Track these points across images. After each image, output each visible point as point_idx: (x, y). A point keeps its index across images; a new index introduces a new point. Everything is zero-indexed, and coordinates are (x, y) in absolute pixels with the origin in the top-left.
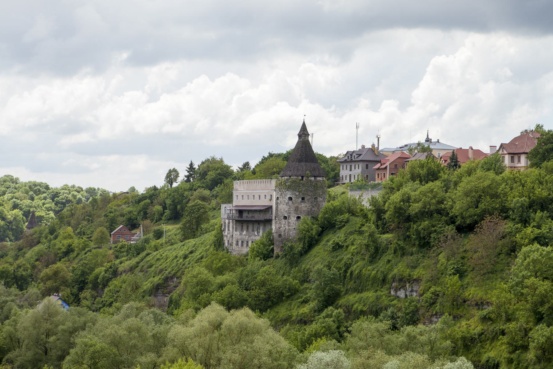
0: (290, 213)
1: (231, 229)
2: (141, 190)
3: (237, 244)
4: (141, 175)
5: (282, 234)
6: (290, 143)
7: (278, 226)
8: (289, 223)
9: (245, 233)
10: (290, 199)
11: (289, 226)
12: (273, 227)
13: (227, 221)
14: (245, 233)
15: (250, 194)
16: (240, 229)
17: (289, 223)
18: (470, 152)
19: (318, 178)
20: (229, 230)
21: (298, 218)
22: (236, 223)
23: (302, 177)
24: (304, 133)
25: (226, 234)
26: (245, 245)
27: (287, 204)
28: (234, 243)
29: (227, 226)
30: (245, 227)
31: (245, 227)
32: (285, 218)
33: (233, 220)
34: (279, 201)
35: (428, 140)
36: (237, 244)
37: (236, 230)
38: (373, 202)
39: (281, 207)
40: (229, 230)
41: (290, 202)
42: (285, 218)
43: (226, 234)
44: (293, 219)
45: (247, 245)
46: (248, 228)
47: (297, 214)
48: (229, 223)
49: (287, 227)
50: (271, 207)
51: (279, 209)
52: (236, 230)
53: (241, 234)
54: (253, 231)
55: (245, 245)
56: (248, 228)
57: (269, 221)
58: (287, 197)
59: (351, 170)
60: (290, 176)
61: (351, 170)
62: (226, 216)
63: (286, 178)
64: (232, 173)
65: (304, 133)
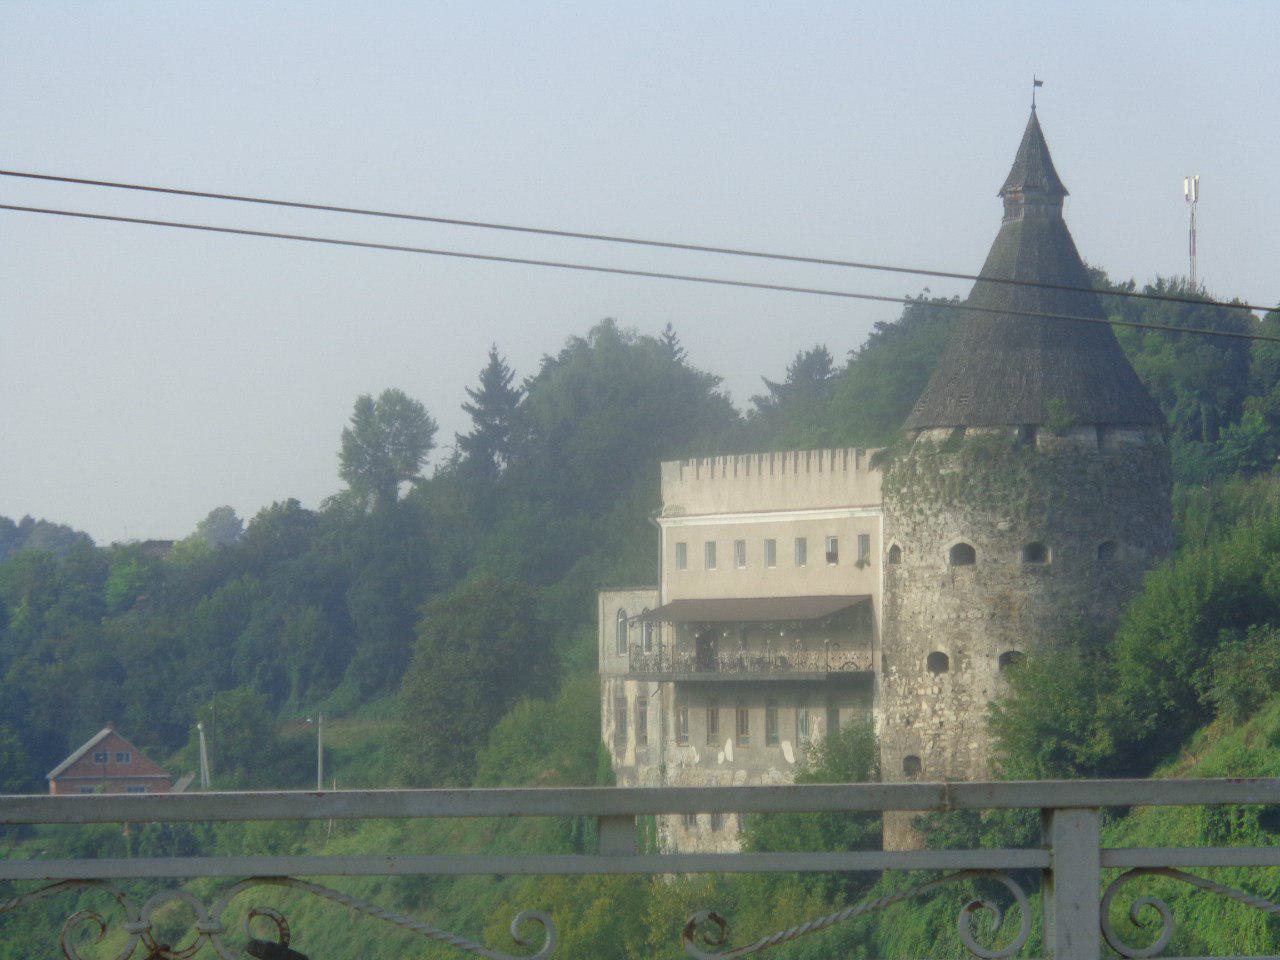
0: (961, 635)
1: (653, 733)
5: (926, 752)
6: (956, 240)
7: (899, 710)
8: (959, 689)
9: (728, 751)
10: (963, 555)
11: (961, 707)
12: (878, 715)
13: (631, 689)
14: (728, 751)
15: (739, 529)
16: (703, 730)
17: (959, 689)
20: (642, 739)
22: (678, 702)
23: (1029, 432)
25: (629, 759)
27: (947, 583)
29: (631, 716)
30: (727, 717)
31: (727, 717)
32: (938, 662)
33: (662, 681)
34: (902, 572)
37: (681, 739)
40: (642, 739)
41: (965, 575)
42: (938, 662)
43: (629, 759)
46: (742, 728)
47: (1004, 638)
48: (642, 702)
49: (950, 716)
50: (864, 604)
51: (904, 615)
52: (681, 739)
54: (772, 739)
56: (742, 728)
57: (857, 687)
58: (946, 548)
62: (623, 663)
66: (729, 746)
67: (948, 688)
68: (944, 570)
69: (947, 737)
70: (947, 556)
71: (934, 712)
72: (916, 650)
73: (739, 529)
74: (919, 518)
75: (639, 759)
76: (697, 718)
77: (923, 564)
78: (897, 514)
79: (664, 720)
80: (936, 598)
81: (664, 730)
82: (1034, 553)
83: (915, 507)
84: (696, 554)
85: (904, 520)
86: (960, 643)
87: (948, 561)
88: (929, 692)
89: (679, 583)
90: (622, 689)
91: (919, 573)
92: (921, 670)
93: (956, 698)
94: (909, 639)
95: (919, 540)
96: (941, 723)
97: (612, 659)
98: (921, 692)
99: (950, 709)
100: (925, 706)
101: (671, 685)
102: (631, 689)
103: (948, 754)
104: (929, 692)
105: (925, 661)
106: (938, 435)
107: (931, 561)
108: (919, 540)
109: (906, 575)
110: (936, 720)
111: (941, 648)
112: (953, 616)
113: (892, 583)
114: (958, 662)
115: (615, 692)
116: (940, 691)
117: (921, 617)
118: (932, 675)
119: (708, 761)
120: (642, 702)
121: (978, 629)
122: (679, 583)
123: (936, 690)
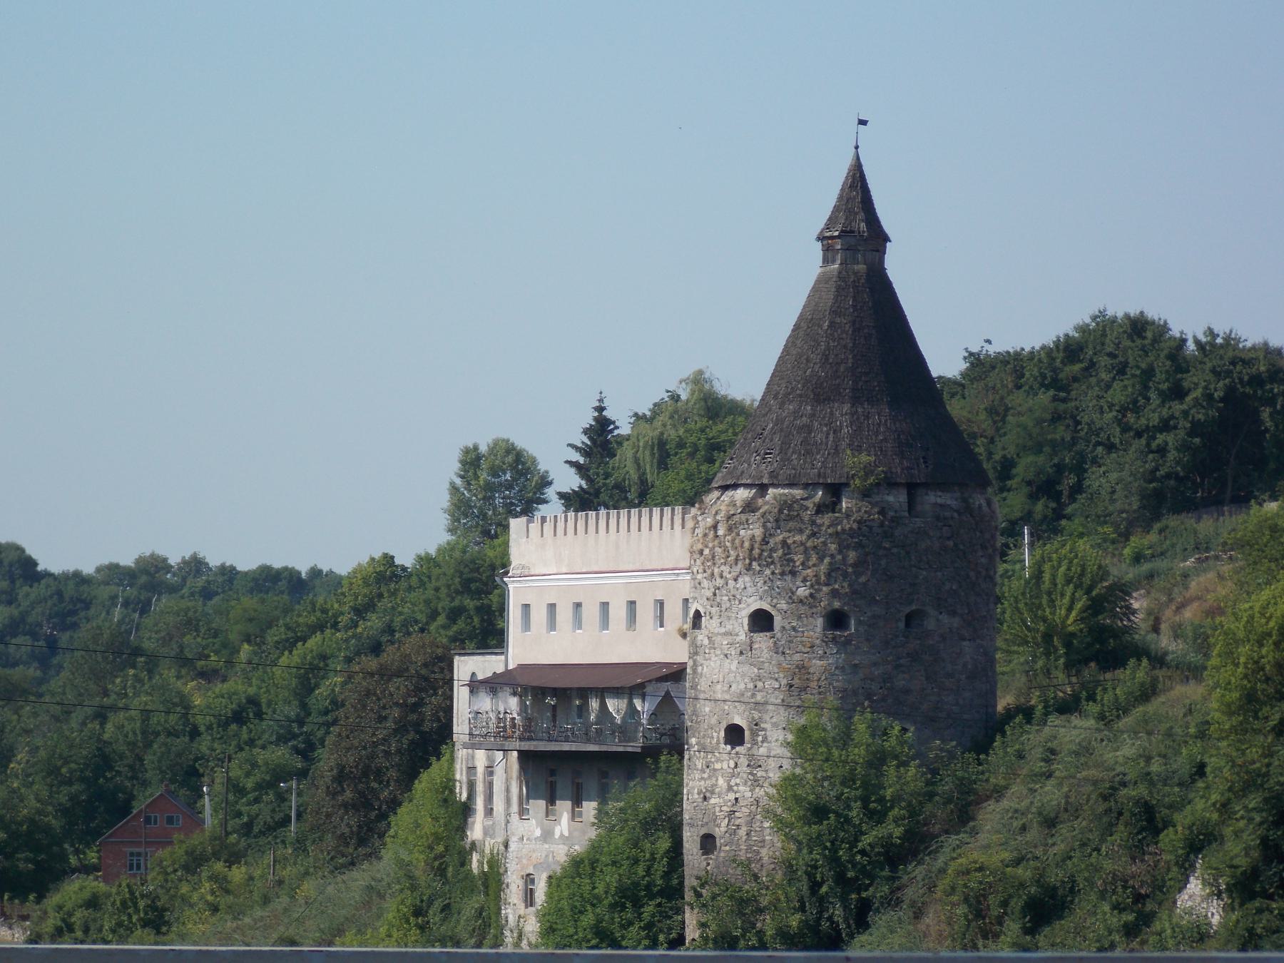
5: (719, 831)
8: (754, 764)
10: (761, 621)
11: (756, 783)
20: (489, 812)
27: (746, 651)
29: (480, 788)
32: (734, 735)
37: (522, 812)
40: (489, 812)
41: (763, 641)
48: (490, 770)
49: (744, 791)
58: (745, 613)
60: (763, 489)
63: (742, 494)
66: (565, 818)
67: (743, 761)
68: (742, 637)
69: (743, 812)
70: (746, 621)
71: (730, 788)
72: (714, 721)
74: (719, 582)
75: (486, 832)
77: (723, 630)
78: (699, 576)
79: (508, 790)
80: (733, 667)
81: (508, 801)
83: (716, 570)
84: (539, 616)
85: (705, 583)
86: (756, 715)
87: (746, 627)
88: (725, 766)
89: (528, 645)
90: (473, 757)
91: (718, 639)
92: (718, 743)
93: (751, 773)
94: (707, 709)
95: (719, 605)
96: (736, 799)
98: (718, 766)
99: (745, 784)
100: (721, 781)
101: (515, 753)
103: (742, 832)
104: (725, 766)
105: (722, 734)
107: (729, 627)
108: (719, 605)
109: (706, 642)
110: (731, 796)
111: (738, 720)
112: (751, 686)
114: (754, 734)
115: (467, 760)
116: (736, 766)
117: (719, 687)
118: (729, 747)
120: (490, 770)
122: (528, 645)
123: (732, 765)
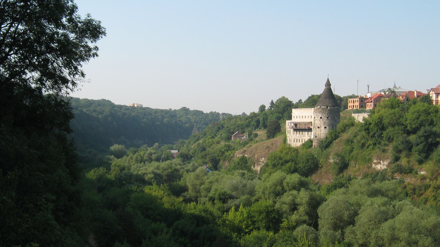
2: (248, 114)
3: (294, 141)
4: (250, 107)
5: (317, 136)
7: (315, 132)
9: (298, 135)
10: (321, 118)
13: (289, 129)
14: (298, 135)
18: (415, 92)
19: (336, 107)
21: (325, 127)
23: (327, 107)
24: (328, 84)
26: (298, 141)
28: (293, 140)
32: (319, 127)
35: (395, 87)
36: (294, 141)
38: (364, 119)
39: (316, 122)
41: (321, 119)
42: (319, 127)
44: (323, 128)
45: (299, 141)
50: (312, 122)
53: (296, 136)
55: (298, 141)
59: (354, 103)
61: (354, 103)
62: (288, 127)
64: (293, 105)
65: (328, 84)
73: (300, 115)
76: (295, 132)
82: (328, 118)
84: (295, 117)
89: (294, 120)
97: (287, 126)
102: (289, 129)
106: (319, 107)
113: (314, 120)
119: (296, 136)
121: (322, 125)
122: (294, 120)
